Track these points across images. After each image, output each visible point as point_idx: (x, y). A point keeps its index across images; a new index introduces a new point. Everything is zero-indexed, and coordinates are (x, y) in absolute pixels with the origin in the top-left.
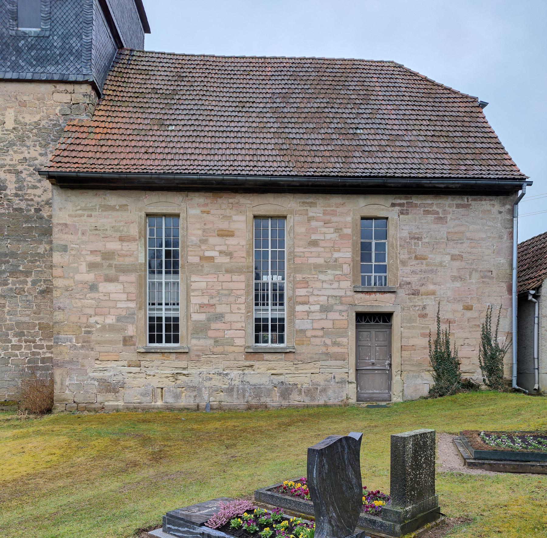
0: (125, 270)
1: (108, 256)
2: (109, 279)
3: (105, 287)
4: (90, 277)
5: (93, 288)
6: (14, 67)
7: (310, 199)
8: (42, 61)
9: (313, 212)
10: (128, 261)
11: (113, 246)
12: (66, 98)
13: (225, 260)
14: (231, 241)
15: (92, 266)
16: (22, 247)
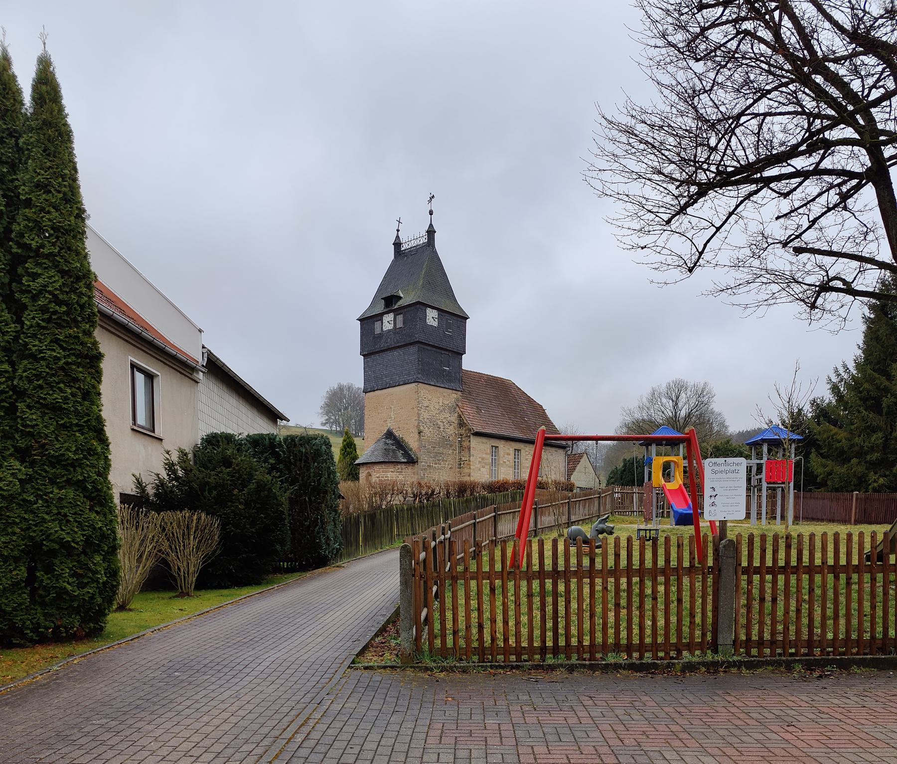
0: (486, 464)
1: (483, 459)
2: (484, 467)
3: (482, 470)
4: (478, 466)
5: (480, 470)
6: (443, 383)
7: (526, 445)
8: (450, 381)
9: (527, 449)
10: (487, 461)
11: (484, 456)
12: (455, 396)
13: (507, 463)
14: (510, 457)
15: (479, 462)
16: (445, 451)
